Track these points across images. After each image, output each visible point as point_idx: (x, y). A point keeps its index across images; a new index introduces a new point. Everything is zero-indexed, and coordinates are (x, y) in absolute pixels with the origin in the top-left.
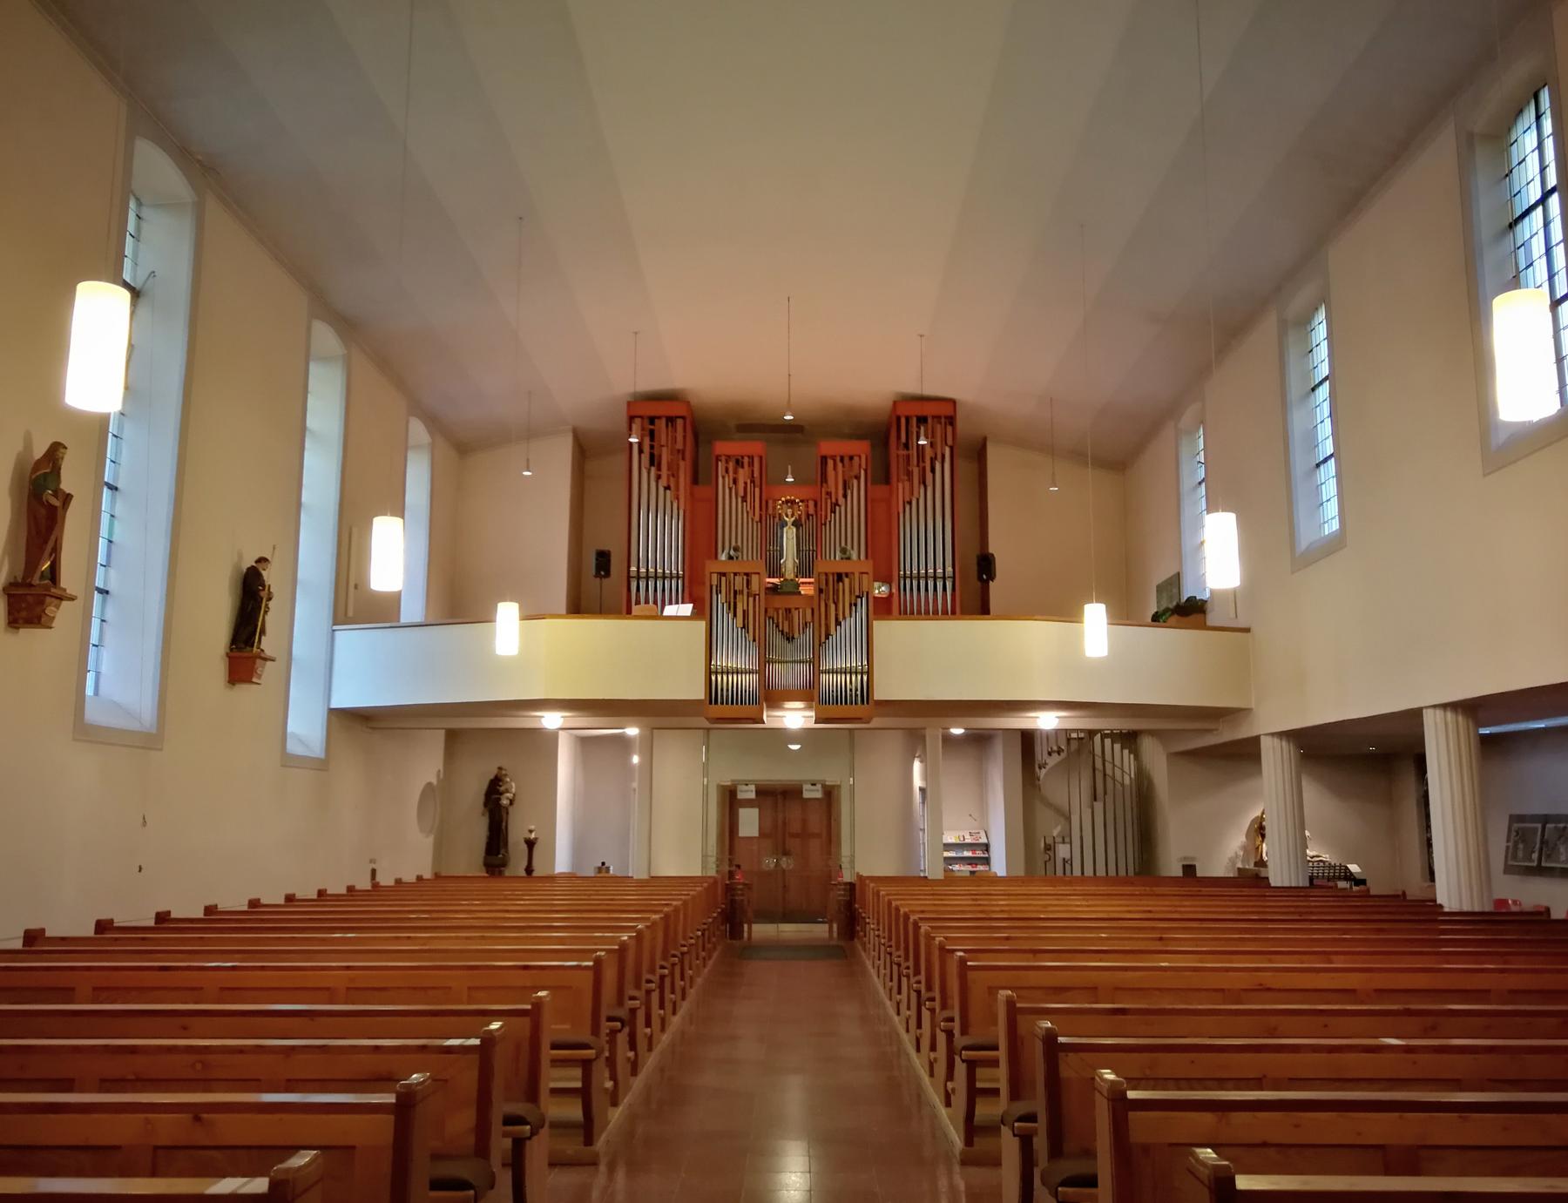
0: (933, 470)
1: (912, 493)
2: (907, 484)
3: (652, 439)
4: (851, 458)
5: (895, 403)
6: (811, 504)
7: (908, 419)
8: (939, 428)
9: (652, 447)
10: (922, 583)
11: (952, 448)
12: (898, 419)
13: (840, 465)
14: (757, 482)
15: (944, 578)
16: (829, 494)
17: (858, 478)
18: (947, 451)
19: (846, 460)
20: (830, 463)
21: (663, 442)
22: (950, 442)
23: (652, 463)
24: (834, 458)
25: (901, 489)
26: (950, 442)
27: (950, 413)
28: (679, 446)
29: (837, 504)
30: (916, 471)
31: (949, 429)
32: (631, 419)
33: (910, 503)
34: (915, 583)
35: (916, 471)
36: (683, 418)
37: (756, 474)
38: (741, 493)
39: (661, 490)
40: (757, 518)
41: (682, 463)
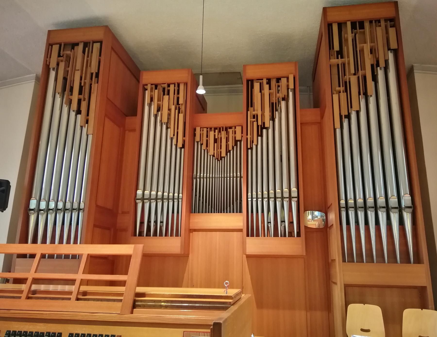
0: (375, 78)
1: (350, 105)
2: (343, 96)
3: (67, 65)
4: (278, 80)
5: (325, 9)
6: (238, 129)
7: (340, 25)
8: (380, 32)
9: (66, 72)
10: (371, 215)
11: (397, 53)
12: (330, 26)
13: (266, 87)
14: (183, 108)
15: (400, 209)
16: (255, 117)
17: (285, 99)
18: (391, 56)
19: (273, 82)
20: (257, 86)
21: (78, 66)
22: (394, 45)
23: (64, 89)
24: (260, 79)
25: (336, 102)
26: (394, 45)
27: (390, 13)
28: (94, 69)
29: (263, 127)
30: (354, 80)
31: (392, 31)
32: (50, 46)
33: (348, 117)
34: (361, 215)
35: (354, 80)
36: (101, 42)
37: (181, 101)
38: (165, 120)
39: (73, 114)
40: (180, 145)
41: (95, 87)
